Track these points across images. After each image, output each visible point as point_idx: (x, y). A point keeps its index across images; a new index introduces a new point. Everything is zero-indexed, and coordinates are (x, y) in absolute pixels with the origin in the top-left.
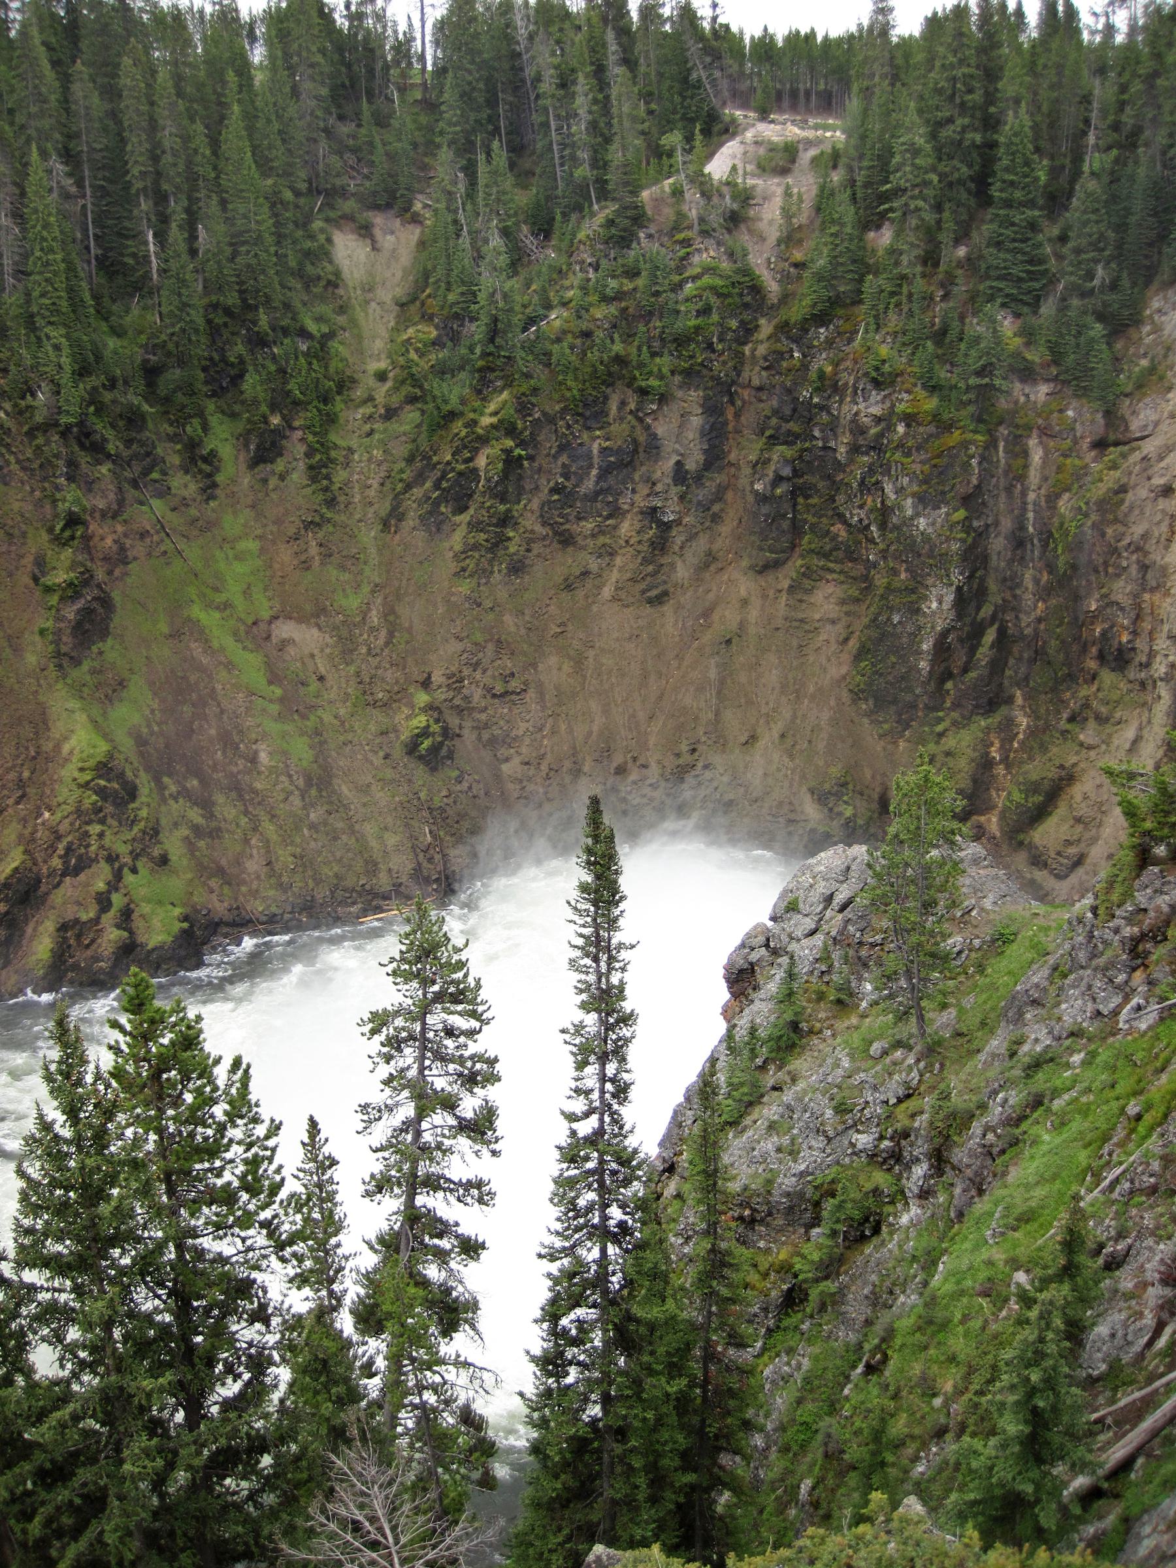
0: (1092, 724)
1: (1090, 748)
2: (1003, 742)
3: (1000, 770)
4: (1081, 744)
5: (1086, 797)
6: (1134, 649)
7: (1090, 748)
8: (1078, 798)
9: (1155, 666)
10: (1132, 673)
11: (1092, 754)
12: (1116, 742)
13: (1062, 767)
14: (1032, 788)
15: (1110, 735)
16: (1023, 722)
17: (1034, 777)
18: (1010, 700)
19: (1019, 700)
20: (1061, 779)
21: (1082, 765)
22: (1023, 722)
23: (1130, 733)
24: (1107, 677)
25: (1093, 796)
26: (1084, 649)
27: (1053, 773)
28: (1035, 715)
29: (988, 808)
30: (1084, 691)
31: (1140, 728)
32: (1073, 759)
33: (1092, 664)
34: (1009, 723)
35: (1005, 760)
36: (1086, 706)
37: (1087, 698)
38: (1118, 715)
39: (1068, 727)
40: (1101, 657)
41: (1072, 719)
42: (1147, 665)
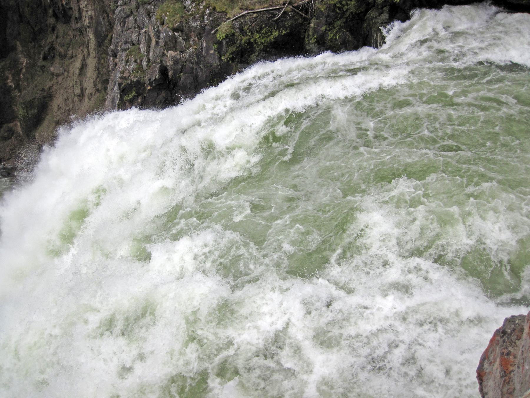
0: (57, 60)
1: (58, 75)
2: (13, 75)
3: (16, 93)
4: (52, 74)
5: (59, 108)
6: (71, 8)
7: (58, 75)
8: (56, 109)
9: (84, 18)
10: (74, 25)
11: (60, 79)
12: (72, 70)
13: (43, 90)
14: (29, 105)
15: (68, 66)
16: (24, 61)
17: (28, 99)
18: (14, 48)
19: (20, 48)
20: (44, 98)
21: (55, 87)
22: (24, 61)
23: (78, 64)
24: (61, 28)
25: (63, 106)
26: (45, 13)
27: (38, 95)
28: (29, 56)
29: (14, 118)
30: (51, 38)
31: (84, 59)
32: (49, 84)
33: (51, 21)
34: (16, 63)
35: (18, 86)
36: (52, 48)
37: (52, 43)
38: (70, 53)
39: (44, 63)
40: (55, 15)
41: (45, 58)
42: (80, 18)
